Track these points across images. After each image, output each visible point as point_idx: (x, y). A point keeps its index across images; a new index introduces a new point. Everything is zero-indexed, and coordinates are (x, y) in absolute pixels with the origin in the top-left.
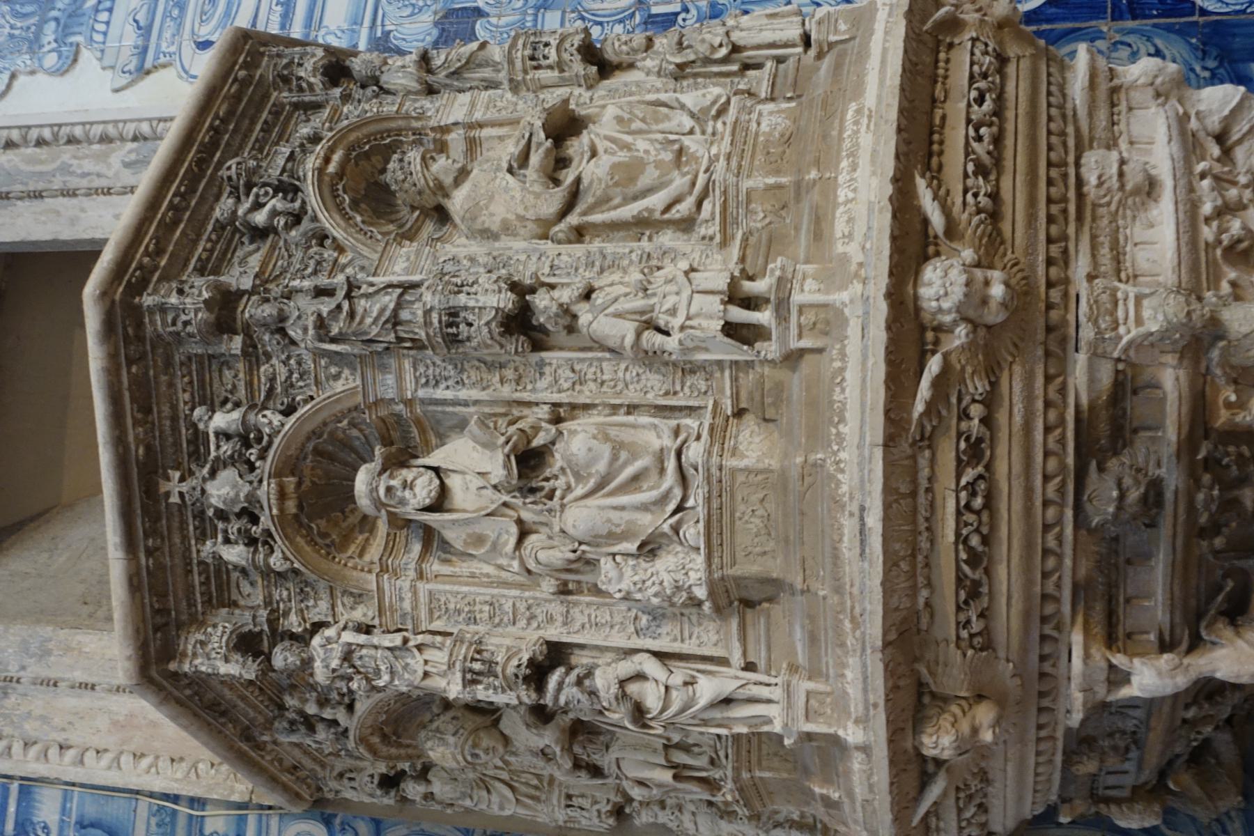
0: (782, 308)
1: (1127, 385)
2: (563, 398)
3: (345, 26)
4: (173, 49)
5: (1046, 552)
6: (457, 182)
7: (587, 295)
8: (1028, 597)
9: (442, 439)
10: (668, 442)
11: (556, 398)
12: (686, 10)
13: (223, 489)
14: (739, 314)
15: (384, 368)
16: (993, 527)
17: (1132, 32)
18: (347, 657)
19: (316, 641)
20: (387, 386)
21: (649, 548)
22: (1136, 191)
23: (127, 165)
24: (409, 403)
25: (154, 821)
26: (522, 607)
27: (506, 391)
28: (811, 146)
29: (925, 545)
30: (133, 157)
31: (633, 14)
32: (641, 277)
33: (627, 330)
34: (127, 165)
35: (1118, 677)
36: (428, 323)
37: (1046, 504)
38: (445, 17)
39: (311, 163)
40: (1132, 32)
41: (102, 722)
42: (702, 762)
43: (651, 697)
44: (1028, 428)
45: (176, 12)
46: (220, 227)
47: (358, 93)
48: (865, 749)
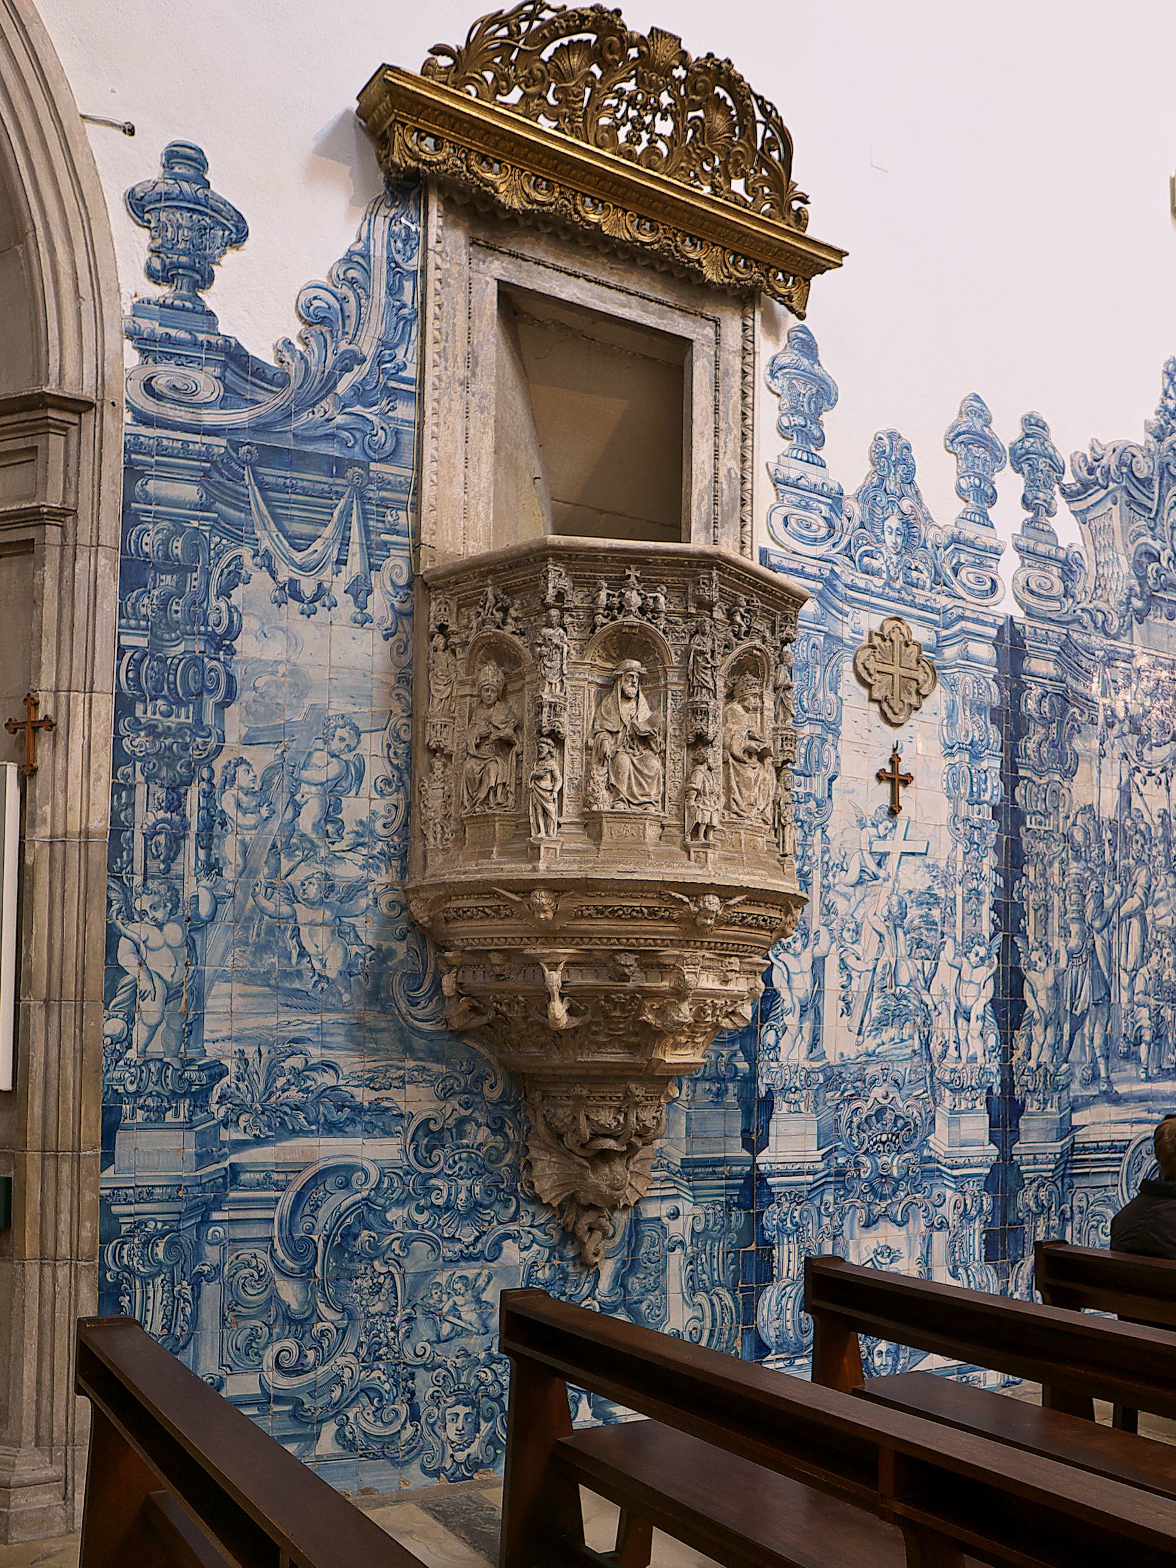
0: (708, 846)
1: (664, 969)
2: (668, 756)
5: (609, 939)
6: (744, 707)
7: (710, 769)
8: (593, 932)
9: (646, 697)
10: (653, 798)
11: (668, 752)
13: (635, 600)
14: (703, 829)
15: (680, 678)
16: (626, 919)
18: (557, 646)
19: (561, 631)
20: (673, 677)
21: (611, 788)
22: (726, 976)
24: (666, 686)
26: (579, 728)
27: (670, 730)
29: (622, 894)
33: (699, 786)
35: (554, 966)
36: (702, 703)
37: (628, 939)
39: (758, 642)
41: (450, 448)
42: (500, 799)
43: (546, 784)
44: (657, 933)
46: (735, 596)
48: (535, 869)
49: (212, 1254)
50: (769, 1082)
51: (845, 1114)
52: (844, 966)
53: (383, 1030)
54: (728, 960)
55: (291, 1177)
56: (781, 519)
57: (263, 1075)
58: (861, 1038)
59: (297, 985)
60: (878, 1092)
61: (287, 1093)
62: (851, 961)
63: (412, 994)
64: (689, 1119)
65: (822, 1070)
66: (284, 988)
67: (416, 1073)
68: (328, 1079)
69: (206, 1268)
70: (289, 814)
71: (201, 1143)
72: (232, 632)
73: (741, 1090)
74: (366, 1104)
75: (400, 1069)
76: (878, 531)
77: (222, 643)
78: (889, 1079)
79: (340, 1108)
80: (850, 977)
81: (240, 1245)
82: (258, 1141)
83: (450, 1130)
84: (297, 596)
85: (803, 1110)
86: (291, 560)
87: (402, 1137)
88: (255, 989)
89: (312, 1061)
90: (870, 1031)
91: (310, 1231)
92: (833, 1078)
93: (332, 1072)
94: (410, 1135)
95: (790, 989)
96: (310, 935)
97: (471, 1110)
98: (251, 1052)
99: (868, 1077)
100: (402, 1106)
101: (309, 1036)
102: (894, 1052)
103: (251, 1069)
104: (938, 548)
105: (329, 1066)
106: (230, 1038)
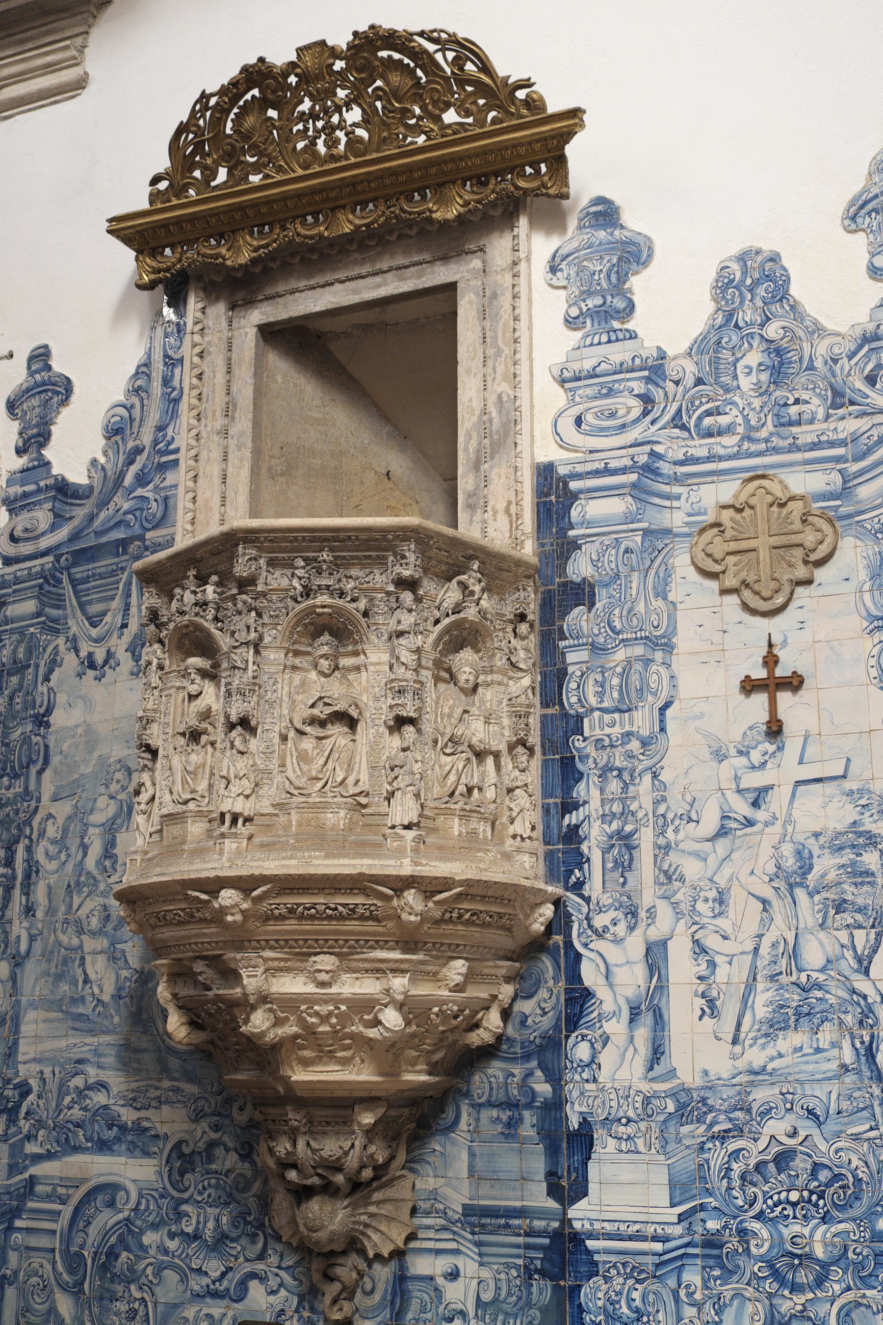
3: (588, 516)
4: (577, 399)
12: (585, 740)
13: (189, 598)
17: (558, 999)
23: (500, 397)
28: (319, 839)
30: (505, 398)
31: (584, 707)
32: (241, 774)
34: (500, 397)
40: (558, 999)
45: (604, 391)
47: (393, 599)
49: (13, 1257)
50: (584, 1109)
51: (717, 1157)
52: (700, 949)
53: (144, 1051)
55: (71, 1191)
56: (571, 421)
58: (738, 1049)
59: (81, 1010)
60: (777, 1127)
61: (71, 1111)
62: (712, 942)
64: (472, 1154)
65: (673, 1095)
66: (72, 1013)
67: (171, 1093)
68: (100, 1098)
69: (8, 1272)
71: (12, 1156)
72: (49, 711)
73: (542, 1119)
74: (130, 1123)
75: (157, 1088)
76: (726, 380)
77: (42, 721)
78: (797, 1108)
79: (110, 1127)
80: (712, 964)
81: (32, 1253)
82: (50, 1156)
84: (92, 665)
85: (641, 1148)
88: (54, 1015)
89: (91, 1081)
90: (755, 1039)
91: (82, 1246)
92: (689, 1106)
93: (104, 1091)
94: (165, 1156)
95: (611, 985)
96: (93, 963)
97: (219, 1134)
98: (47, 1071)
99: (755, 1107)
100: (158, 1126)
101: (89, 1057)
102: (804, 1067)
103: (47, 1088)
104: (835, 361)
105: (102, 1086)
106: (34, 1060)
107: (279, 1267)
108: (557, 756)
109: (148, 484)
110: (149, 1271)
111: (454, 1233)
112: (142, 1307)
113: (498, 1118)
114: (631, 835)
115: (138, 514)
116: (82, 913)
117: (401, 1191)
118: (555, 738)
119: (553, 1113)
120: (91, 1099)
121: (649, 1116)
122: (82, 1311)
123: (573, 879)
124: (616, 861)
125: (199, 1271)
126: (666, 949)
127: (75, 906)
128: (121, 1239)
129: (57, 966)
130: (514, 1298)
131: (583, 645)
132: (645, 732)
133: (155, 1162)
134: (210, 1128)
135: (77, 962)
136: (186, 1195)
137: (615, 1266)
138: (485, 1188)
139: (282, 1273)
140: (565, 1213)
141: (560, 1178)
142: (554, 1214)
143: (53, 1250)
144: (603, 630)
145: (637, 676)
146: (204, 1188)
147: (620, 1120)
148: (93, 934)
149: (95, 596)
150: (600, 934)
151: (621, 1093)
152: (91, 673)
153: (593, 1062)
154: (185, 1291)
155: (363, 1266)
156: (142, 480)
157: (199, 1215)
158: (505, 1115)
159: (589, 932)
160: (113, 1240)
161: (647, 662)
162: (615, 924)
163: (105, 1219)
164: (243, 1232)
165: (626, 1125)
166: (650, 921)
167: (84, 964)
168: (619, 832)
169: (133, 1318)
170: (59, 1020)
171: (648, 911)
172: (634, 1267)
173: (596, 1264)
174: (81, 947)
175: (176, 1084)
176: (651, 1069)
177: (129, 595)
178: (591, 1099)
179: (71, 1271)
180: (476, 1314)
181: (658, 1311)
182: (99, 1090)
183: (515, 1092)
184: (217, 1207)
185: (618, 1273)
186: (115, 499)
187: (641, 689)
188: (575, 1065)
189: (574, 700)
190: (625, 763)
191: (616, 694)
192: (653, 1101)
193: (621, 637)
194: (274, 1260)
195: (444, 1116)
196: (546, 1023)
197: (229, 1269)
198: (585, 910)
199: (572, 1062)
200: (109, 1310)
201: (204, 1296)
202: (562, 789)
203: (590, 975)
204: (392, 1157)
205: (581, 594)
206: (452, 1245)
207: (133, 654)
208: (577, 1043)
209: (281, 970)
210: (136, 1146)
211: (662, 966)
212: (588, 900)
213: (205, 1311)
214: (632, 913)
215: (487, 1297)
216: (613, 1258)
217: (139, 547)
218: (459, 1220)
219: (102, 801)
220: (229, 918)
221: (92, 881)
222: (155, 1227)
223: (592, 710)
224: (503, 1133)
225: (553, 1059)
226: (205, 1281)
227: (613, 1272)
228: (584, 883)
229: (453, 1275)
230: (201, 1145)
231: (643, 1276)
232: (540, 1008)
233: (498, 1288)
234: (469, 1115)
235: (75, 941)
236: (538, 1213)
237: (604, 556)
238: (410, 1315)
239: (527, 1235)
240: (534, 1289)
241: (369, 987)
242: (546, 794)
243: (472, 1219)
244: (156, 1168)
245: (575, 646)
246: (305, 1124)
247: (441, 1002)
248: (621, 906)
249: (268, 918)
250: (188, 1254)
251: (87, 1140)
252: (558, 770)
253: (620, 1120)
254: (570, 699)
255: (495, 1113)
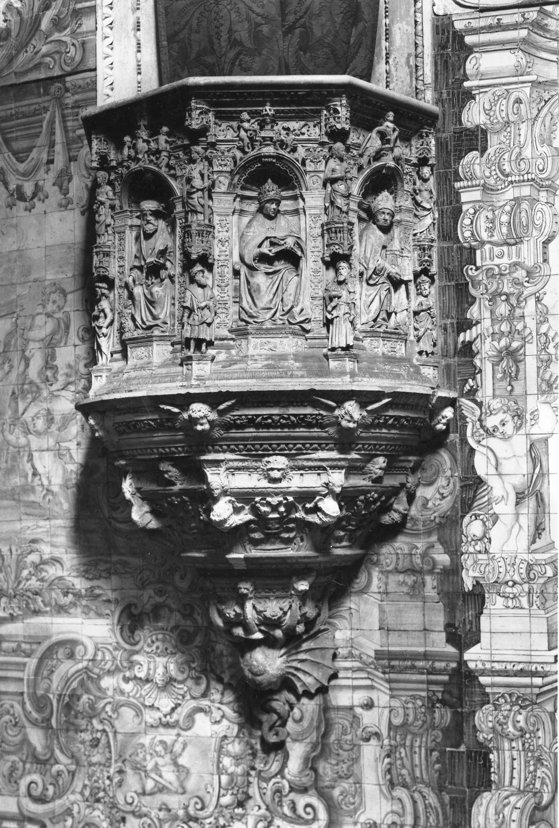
12: (477, 269)
25: (89, 80)
31: (476, 241)
38: (482, 129)
40: (454, 485)
50: (477, 574)
54: (266, 459)
55: (34, 647)
57: (13, 567)
59: (32, 498)
61: (29, 582)
63: (111, 500)
64: (382, 611)
70: (22, 368)
73: (441, 582)
74: (83, 591)
75: (106, 562)
79: (66, 594)
83: (147, 614)
84: (22, 197)
86: (17, 171)
87: (111, 618)
89: (46, 557)
93: (58, 565)
96: (40, 458)
97: (164, 598)
103: (6, 563)
105: (55, 560)
107: (221, 703)
108: (453, 283)
109: (65, 28)
110: (108, 708)
111: (369, 673)
112: (104, 737)
113: (404, 583)
114: (517, 350)
115: (57, 57)
116: (28, 416)
117: (323, 641)
118: (451, 267)
119: (451, 578)
120: (46, 571)
121: (532, 580)
122: (52, 740)
123: (467, 387)
124: (504, 372)
125: (152, 707)
126: (547, 445)
127: (21, 410)
128: (82, 684)
129: (6, 462)
130: (420, 722)
131: (476, 186)
132: (529, 263)
133: (108, 621)
134: (155, 593)
135: (26, 458)
136: (137, 648)
137: (503, 696)
138: (393, 638)
139: (224, 707)
140: (461, 655)
141: (457, 629)
142: (452, 657)
143: (22, 694)
144: (493, 173)
145: (523, 214)
146: (153, 642)
147: (507, 583)
148: (38, 434)
149: (19, 133)
150: (490, 433)
151: (508, 561)
152: (22, 205)
153: (485, 537)
154: (140, 724)
155: (292, 698)
156: (58, 24)
157: (149, 663)
158: (410, 579)
159: (482, 431)
160: (75, 685)
161: (534, 201)
162: (504, 425)
163: (66, 668)
164: (188, 676)
165: (513, 586)
166: (533, 422)
167: (32, 460)
168: (507, 348)
169: (96, 746)
170: (12, 507)
171: (532, 413)
172: (519, 697)
173: (487, 695)
174: (28, 445)
175: (123, 558)
176: (534, 542)
177: (52, 133)
178: (483, 566)
179: (39, 709)
180: (389, 735)
181: (538, 730)
182: (53, 564)
183: (419, 561)
184: (165, 656)
185: (506, 702)
186: (33, 42)
187: (527, 226)
188: (469, 539)
189: (467, 234)
190: (512, 289)
191: (504, 230)
192: (535, 567)
193: (510, 179)
194: (217, 696)
195: (358, 581)
196: (445, 505)
197: (177, 706)
198: (478, 413)
199: (467, 537)
200: (74, 739)
201: (157, 727)
202: (457, 311)
203: (482, 465)
204: (319, 615)
205: (475, 139)
206: (368, 682)
207: (61, 188)
208: (471, 522)
209: (238, 469)
210: (91, 609)
211: (544, 459)
212: (480, 405)
213: (159, 738)
214: (519, 415)
215: (397, 721)
216: (502, 690)
217: (60, 89)
218: (372, 663)
219: (40, 320)
220: (199, 428)
221: (34, 389)
222: (110, 673)
223: (483, 243)
224: (408, 594)
225: (450, 534)
226: (157, 715)
227: (502, 701)
228: (477, 390)
229: (369, 706)
230: (148, 607)
231: (527, 703)
232: (439, 493)
233: (406, 715)
234: (380, 579)
235: (23, 441)
236: (439, 656)
237: (495, 105)
238: (333, 738)
239: (429, 673)
240: (437, 715)
241: (311, 481)
242: (445, 315)
243: (385, 662)
244: (109, 627)
245: (469, 187)
246: (251, 592)
247: (365, 492)
248: (509, 409)
249: (228, 427)
250: (141, 695)
251: (45, 605)
252: (453, 294)
253: (507, 583)
254: (464, 233)
255: (401, 577)
